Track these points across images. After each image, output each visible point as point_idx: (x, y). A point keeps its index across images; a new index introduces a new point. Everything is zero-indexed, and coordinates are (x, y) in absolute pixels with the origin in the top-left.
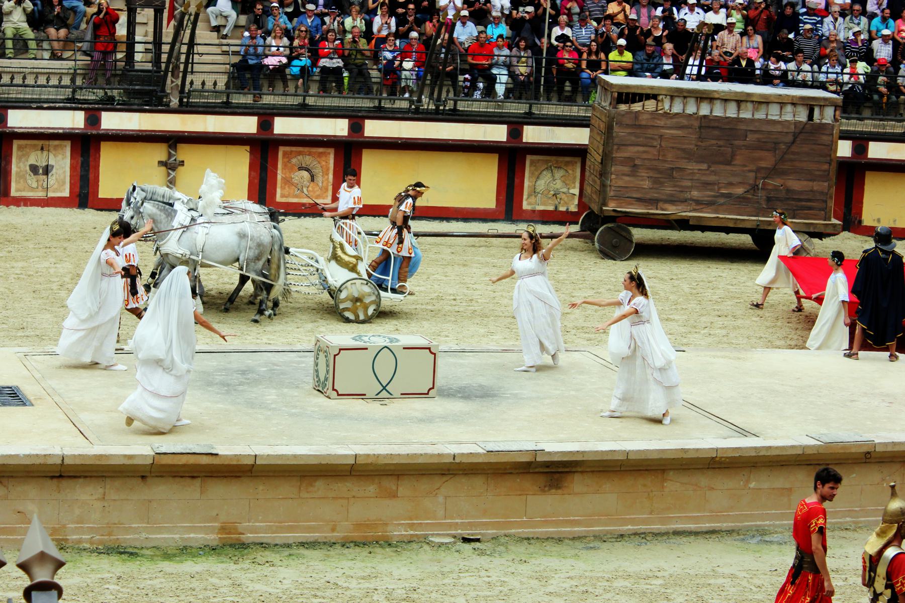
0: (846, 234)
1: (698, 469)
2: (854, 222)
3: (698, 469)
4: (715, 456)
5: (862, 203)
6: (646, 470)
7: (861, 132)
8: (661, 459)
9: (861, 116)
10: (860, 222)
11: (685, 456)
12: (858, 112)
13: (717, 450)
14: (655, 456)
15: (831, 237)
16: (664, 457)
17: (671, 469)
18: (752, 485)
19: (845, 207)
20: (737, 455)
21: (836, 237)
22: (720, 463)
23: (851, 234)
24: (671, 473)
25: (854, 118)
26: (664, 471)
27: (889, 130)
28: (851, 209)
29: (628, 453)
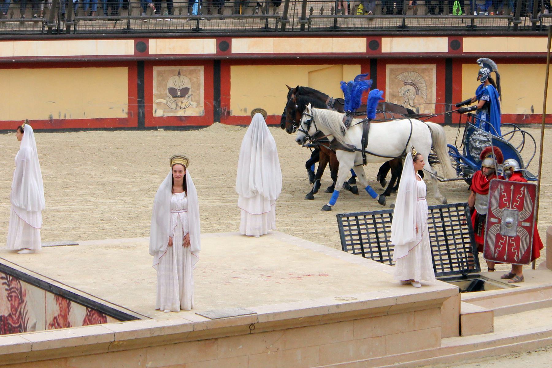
0: (216, 125)
1: (99, 354)
2: (224, 113)
3: (99, 354)
4: (113, 340)
5: (229, 95)
6: (50, 360)
7: (224, 31)
8: (63, 348)
9: (222, 16)
10: (229, 113)
11: (86, 343)
12: (219, 12)
13: (115, 334)
14: (58, 346)
15: (204, 129)
16: (66, 346)
17: (73, 357)
18: (149, 364)
19: (214, 100)
20: (134, 338)
21: (208, 128)
22: (118, 346)
23: (221, 125)
24: (74, 360)
25: (215, 18)
26: (66, 359)
27: (248, 27)
28: (220, 101)
29: (32, 345)
